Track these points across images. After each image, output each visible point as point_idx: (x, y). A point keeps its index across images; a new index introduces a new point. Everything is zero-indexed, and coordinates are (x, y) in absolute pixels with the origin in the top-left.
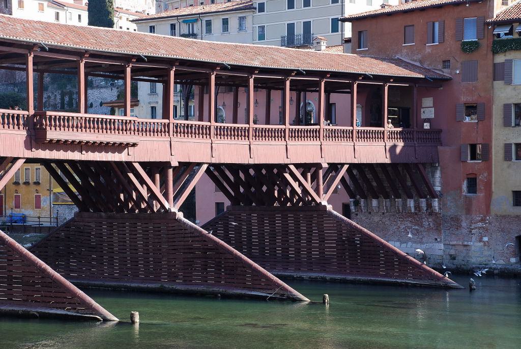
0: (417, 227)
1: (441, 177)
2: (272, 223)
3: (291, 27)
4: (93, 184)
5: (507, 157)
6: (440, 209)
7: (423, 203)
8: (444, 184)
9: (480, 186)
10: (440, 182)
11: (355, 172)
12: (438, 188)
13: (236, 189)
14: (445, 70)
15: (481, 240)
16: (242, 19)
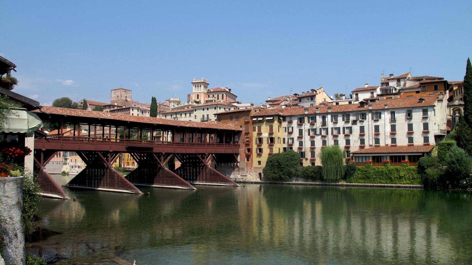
1: (240, 157)
2: (193, 170)
3: (203, 116)
4: (145, 158)
6: (240, 166)
8: (240, 159)
9: (250, 159)
10: (240, 159)
11: (217, 156)
12: (239, 160)
13: (183, 161)
14: (241, 128)
15: (250, 174)
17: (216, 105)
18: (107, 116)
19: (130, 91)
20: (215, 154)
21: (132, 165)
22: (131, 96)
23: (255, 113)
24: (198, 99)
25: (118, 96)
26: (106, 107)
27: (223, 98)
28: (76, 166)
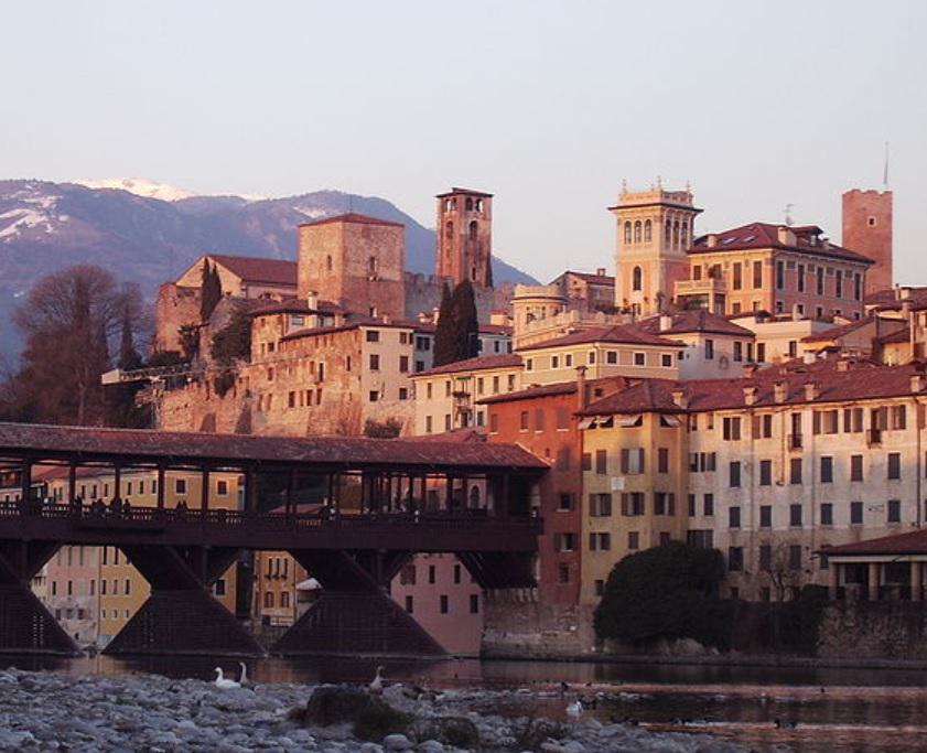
0: (524, 617)
1: (542, 566)
5: (593, 547)
7: (528, 590)
8: (541, 575)
12: (538, 578)
15: (568, 630)
16: (511, 377)
17: (590, 345)
18: (19, 435)
19: (396, 230)
20: (483, 554)
21: (282, 605)
22: (402, 253)
23: (599, 399)
24: (639, 289)
25: (329, 258)
26: (267, 318)
27: (758, 283)
28: (69, 611)
